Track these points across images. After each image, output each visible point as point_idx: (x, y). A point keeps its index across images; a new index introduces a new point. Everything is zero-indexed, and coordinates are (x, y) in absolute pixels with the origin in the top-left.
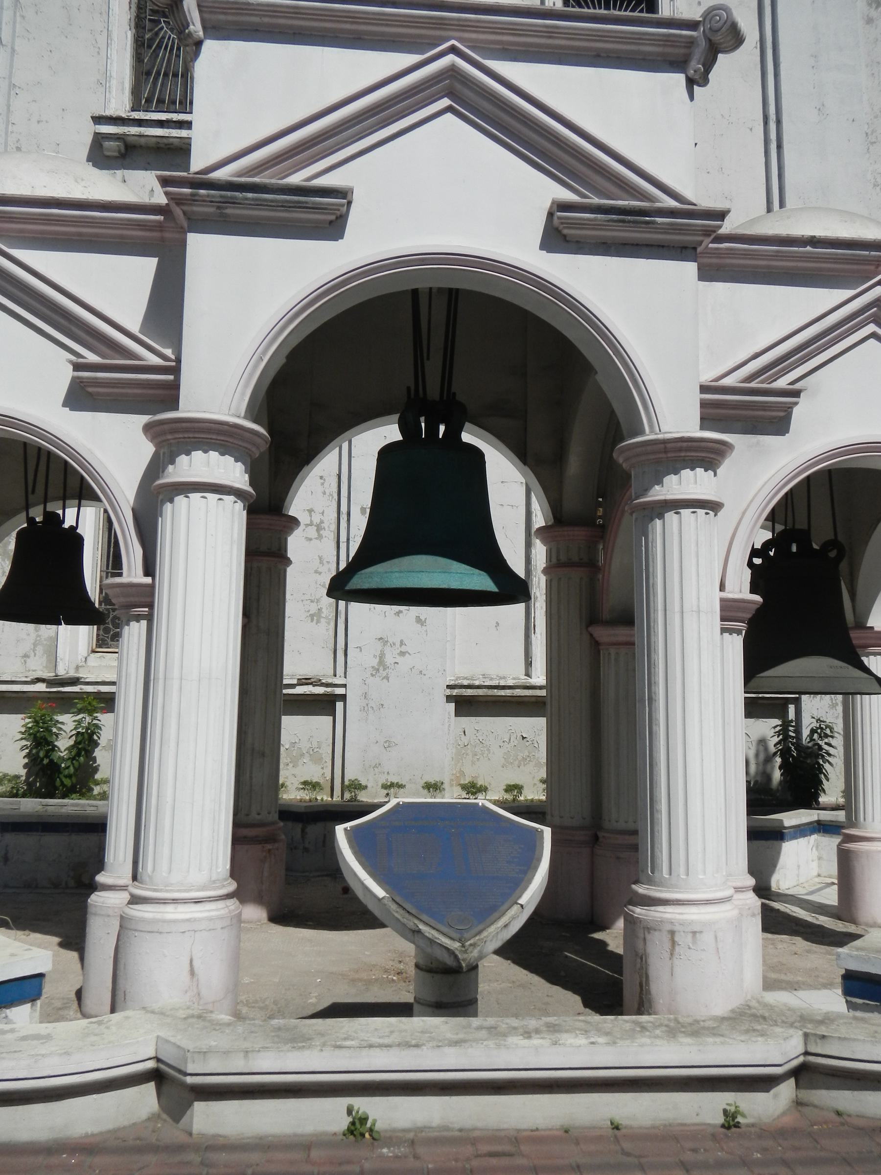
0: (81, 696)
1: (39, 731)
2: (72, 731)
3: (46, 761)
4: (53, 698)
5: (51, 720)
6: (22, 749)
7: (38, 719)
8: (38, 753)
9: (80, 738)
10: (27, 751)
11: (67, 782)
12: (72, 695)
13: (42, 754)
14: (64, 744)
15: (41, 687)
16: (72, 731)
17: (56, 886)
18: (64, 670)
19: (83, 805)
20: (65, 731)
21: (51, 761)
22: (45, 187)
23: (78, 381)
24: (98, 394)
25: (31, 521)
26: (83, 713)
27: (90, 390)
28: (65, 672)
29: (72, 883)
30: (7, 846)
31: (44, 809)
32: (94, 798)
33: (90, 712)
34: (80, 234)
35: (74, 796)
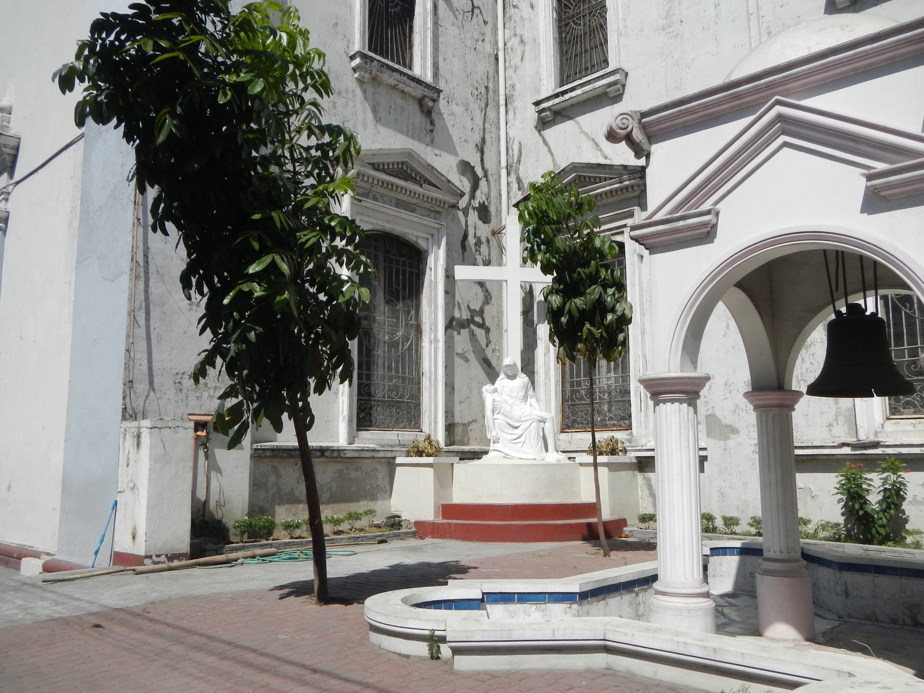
0: (883, 457)
1: (851, 487)
2: (879, 487)
3: (861, 513)
4: (859, 459)
5: (861, 478)
6: (839, 502)
7: (849, 477)
8: (853, 505)
9: (888, 494)
10: (843, 503)
11: (882, 531)
12: (875, 456)
13: (857, 506)
14: (874, 498)
15: (847, 450)
16: (879, 487)
17: (894, 621)
18: (865, 435)
19: (901, 553)
20: (874, 487)
21: (866, 512)
22: (818, 44)
23: (872, 189)
24: (891, 195)
25: (838, 313)
26: (889, 471)
27: (883, 193)
28: (866, 437)
29: (908, 621)
30: (846, 583)
31: (866, 554)
32: (908, 546)
33: (895, 470)
34: (855, 69)
35: (889, 543)
